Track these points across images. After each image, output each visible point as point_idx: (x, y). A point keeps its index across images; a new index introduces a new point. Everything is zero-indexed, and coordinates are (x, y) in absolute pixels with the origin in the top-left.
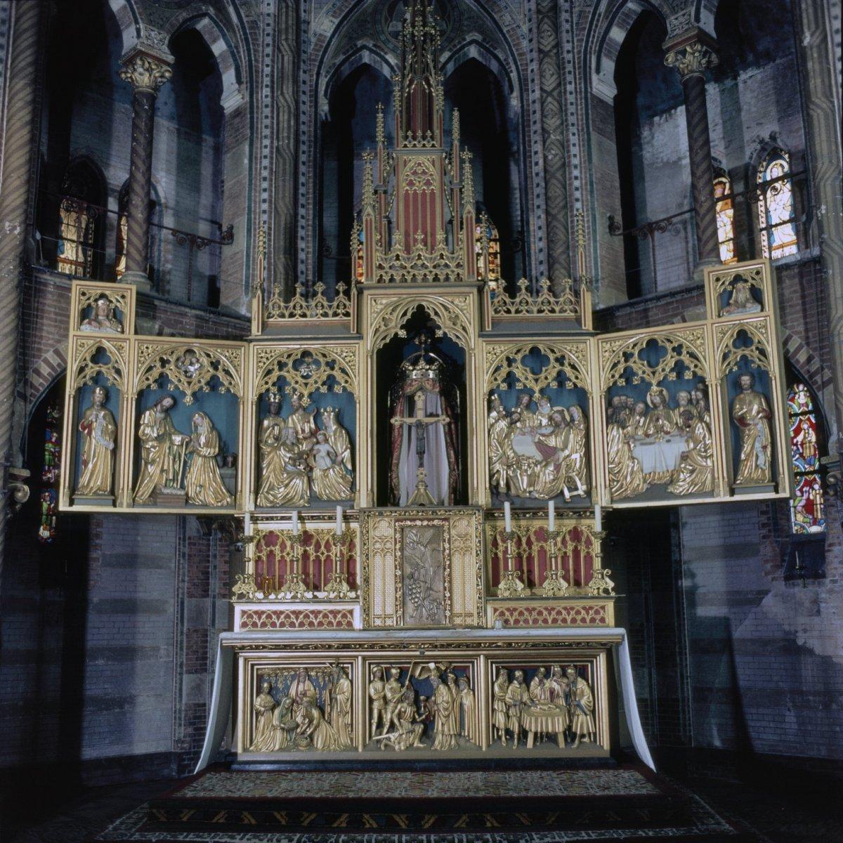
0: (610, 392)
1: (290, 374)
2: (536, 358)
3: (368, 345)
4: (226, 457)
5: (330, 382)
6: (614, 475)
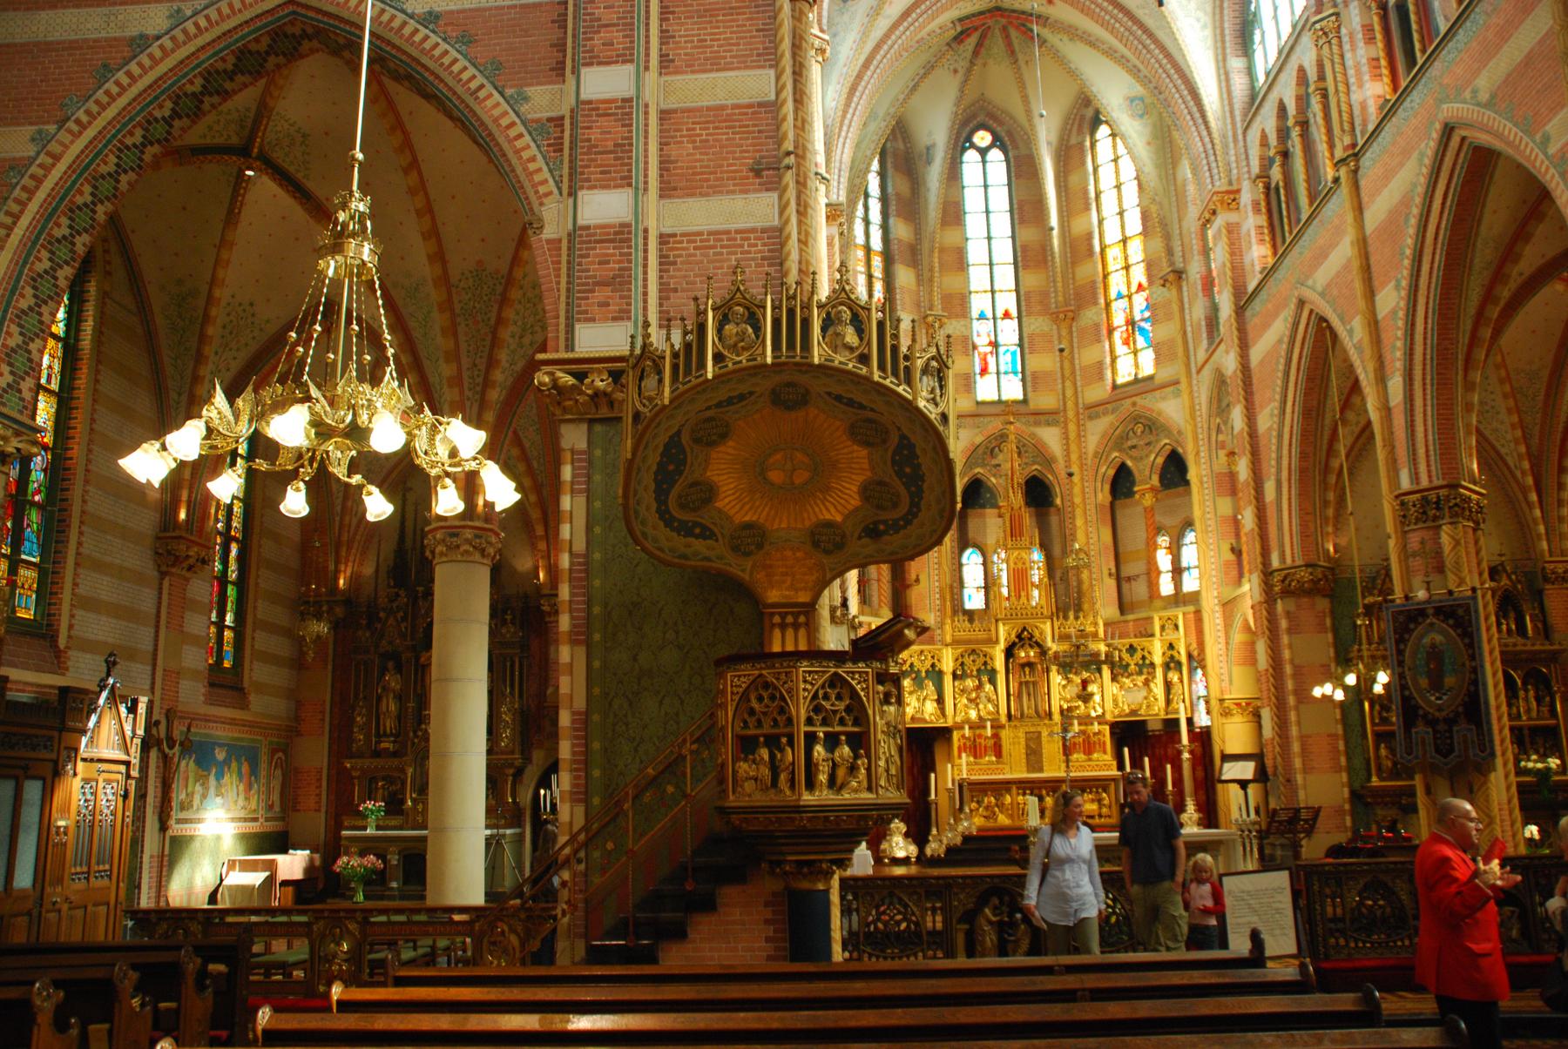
3: (1002, 645)
4: (940, 701)
5: (985, 663)
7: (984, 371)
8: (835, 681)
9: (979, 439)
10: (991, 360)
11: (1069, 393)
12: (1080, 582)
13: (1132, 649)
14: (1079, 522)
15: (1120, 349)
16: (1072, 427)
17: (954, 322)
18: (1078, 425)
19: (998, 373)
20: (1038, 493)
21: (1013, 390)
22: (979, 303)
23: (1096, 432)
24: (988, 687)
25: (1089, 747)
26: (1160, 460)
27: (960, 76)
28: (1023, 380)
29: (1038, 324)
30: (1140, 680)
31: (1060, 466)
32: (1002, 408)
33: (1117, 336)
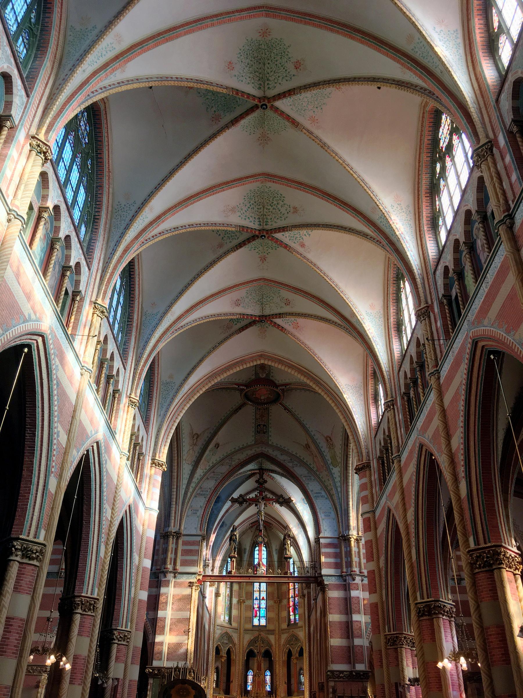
7: (256, 616)
12: (276, 686)
16: (277, 636)
18: (279, 635)
19: (259, 617)
20: (268, 655)
21: (263, 622)
22: (256, 595)
23: (284, 637)
26: (299, 649)
27: (253, 533)
28: (266, 619)
29: (271, 603)
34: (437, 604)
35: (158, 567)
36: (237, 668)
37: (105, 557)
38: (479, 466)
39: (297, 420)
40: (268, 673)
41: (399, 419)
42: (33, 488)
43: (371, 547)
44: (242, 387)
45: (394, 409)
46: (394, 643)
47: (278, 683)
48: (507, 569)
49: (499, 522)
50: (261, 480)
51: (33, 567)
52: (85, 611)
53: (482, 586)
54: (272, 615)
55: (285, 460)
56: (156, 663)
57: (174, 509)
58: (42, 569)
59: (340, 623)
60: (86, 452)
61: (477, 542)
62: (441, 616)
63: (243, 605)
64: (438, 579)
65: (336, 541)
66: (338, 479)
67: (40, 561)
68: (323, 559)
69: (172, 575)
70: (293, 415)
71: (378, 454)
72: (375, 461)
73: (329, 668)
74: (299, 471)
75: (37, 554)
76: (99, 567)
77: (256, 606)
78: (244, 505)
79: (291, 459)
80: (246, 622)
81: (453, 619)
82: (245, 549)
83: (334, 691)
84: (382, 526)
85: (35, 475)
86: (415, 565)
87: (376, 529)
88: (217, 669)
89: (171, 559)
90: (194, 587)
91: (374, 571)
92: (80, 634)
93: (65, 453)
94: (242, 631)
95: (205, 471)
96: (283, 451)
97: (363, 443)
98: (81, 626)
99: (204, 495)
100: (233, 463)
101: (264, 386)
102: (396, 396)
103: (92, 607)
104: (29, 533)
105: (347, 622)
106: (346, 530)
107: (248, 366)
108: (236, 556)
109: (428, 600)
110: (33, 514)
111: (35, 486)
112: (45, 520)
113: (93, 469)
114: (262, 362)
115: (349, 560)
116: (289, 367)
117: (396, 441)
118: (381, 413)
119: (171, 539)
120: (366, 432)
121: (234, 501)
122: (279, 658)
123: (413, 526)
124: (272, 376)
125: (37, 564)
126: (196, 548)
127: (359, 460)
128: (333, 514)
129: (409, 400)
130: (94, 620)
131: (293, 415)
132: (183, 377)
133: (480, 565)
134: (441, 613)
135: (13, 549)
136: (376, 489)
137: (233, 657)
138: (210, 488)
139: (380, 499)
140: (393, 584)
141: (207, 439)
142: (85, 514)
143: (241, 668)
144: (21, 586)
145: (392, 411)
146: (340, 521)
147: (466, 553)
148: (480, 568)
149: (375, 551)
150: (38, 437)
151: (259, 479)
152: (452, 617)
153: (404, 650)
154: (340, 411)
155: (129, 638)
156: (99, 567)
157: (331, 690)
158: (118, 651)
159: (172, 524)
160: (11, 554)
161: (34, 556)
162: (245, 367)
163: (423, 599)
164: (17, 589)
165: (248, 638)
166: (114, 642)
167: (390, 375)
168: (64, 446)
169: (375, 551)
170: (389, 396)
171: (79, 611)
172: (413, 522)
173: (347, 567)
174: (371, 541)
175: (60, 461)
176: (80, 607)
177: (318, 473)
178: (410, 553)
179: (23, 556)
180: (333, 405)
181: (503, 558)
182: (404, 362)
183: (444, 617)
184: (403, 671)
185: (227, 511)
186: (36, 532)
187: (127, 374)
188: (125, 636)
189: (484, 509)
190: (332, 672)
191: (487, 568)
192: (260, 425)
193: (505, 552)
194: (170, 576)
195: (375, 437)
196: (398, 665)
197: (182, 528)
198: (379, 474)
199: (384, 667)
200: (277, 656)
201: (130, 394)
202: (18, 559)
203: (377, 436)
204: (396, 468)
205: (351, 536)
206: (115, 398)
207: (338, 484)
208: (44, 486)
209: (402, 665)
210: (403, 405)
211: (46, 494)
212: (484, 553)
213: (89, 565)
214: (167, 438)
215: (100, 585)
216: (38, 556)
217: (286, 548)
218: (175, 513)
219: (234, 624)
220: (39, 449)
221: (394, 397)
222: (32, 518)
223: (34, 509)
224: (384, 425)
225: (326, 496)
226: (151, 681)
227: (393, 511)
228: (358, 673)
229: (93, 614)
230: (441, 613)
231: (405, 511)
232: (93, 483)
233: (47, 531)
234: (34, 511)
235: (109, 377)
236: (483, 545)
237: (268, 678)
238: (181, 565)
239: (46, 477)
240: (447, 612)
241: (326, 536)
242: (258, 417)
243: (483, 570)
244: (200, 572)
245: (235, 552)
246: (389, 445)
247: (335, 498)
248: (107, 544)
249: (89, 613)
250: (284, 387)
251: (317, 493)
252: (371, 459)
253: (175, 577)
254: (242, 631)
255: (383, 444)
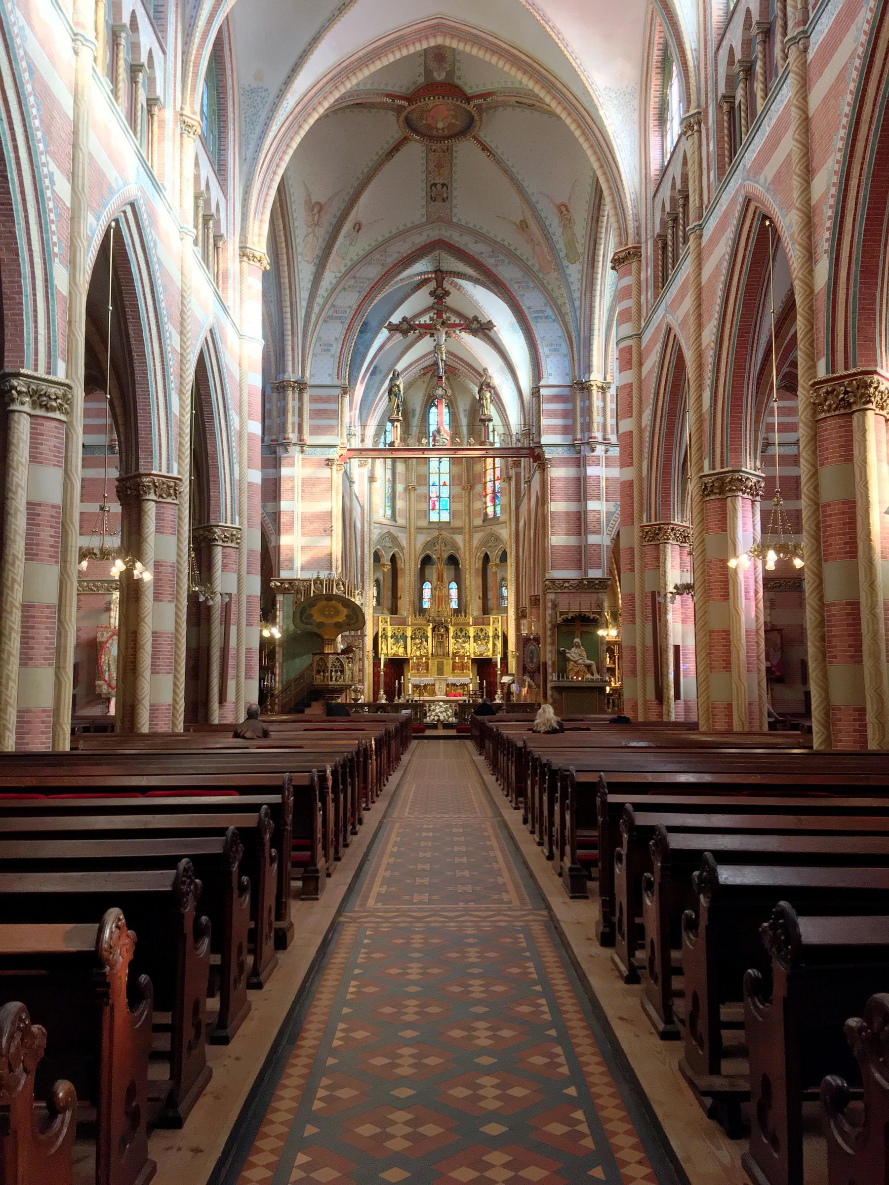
0: (474, 637)
1: (417, 632)
2: (461, 630)
4: (405, 648)
6: (474, 653)
8: (337, 659)
9: (428, 540)
10: (437, 504)
11: (467, 521)
13: (482, 630)
14: (467, 576)
15: (489, 504)
16: (467, 535)
17: (422, 488)
20: (453, 561)
21: (445, 517)
22: (434, 479)
23: (477, 537)
24: (425, 643)
25: (463, 667)
26: (500, 553)
29: (457, 489)
30: (484, 642)
31: (462, 551)
32: (440, 525)
33: (488, 498)
34: (737, 476)
35: (274, 437)
36: (407, 579)
37: (181, 414)
38: (860, 226)
39: (506, 171)
40: (454, 585)
41: (708, 152)
42: (26, 283)
43: (630, 395)
44: (399, 102)
45: (700, 131)
46: (655, 537)
47: (468, 598)
48: (877, 411)
49: (878, 330)
50: (439, 291)
51: (55, 424)
52: (161, 496)
53: (827, 439)
54: (459, 506)
55: (482, 253)
56: (284, 574)
57: (290, 343)
58: (73, 426)
59: (567, 513)
60: (113, 224)
61: (832, 366)
62: (740, 494)
63: (412, 493)
64: (743, 438)
65: (566, 391)
66: (576, 286)
67: (67, 413)
68: (545, 422)
69: (298, 448)
70: (498, 162)
71: (657, 230)
72: (650, 244)
73: (548, 576)
74: (507, 272)
75: (59, 401)
76: (174, 430)
77: (433, 495)
78: (411, 335)
79: (493, 251)
80: (418, 517)
81: (758, 498)
82: (414, 411)
83: (555, 606)
84: (652, 360)
85: (23, 259)
86: (707, 417)
87: (641, 364)
88: (377, 583)
89: (293, 424)
90: (334, 467)
91: (631, 432)
92: (159, 530)
93: (72, 219)
94: (413, 530)
95: (339, 275)
96: (479, 236)
97: (630, 211)
98: (159, 517)
99: (340, 318)
100: (389, 260)
101: (443, 97)
102: (707, 103)
103: (172, 491)
104: (36, 365)
105: (579, 513)
106: (584, 374)
107: (412, 50)
108: (401, 418)
109: (723, 470)
110: (36, 332)
111: (29, 281)
112: (61, 343)
113: (134, 256)
114: (440, 41)
115: (587, 420)
116: (494, 53)
117: (697, 197)
118: (669, 148)
119: (290, 393)
120: (638, 188)
121: (393, 328)
122: (470, 565)
123: (711, 352)
124: (459, 78)
125: (63, 418)
126: (333, 406)
127: (621, 243)
128: (564, 348)
129: (732, 111)
130: (179, 509)
131: (498, 162)
132: (282, 77)
133: (830, 406)
134: (742, 490)
135: (14, 392)
136: (648, 295)
137: (400, 565)
138: (350, 307)
139: (655, 311)
140: (662, 452)
141: (338, 214)
142: (133, 341)
143: (413, 579)
144: (42, 453)
145: (696, 135)
146: (576, 358)
147: (807, 387)
148: (829, 411)
149: (635, 400)
150: (13, 184)
151: (436, 290)
152: (757, 495)
153: (669, 546)
154: (592, 146)
155: (239, 539)
156: (174, 430)
157: (550, 605)
158: (224, 556)
159: (290, 369)
160: (13, 400)
161: (54, 404)
162: (405, 52)
163: (714, 469)
164: (34, 458)
165: (421, 539)
166: (216, 543)
167: (698, 59)
168: (69, 205)
169: (635, 400)
170: (693, 104)
171: (152, 496)
172: (713, 345)
173: (582, 432)
174: (630, 385)
175: (66, 232)
176: (152, 491)
177: (541, 275)
178: (700, 397)
179: (34, 404)
180: (577, 133)
181: (874, 393)
182: (731, 26)
183: (745, 496)
184: (665, 576)
185: (381, 347)
186: (49, 363)
187: (170, 64)
188: (232, 535)
189: (854, 308)
190: (553, 581)
191: (842, 411)
192: (435, 185)
193: (879, 383)
194: (294, 451)
195: (654, 197)
196: (657, 568)
197: (307, 374)
198: (656, 266)
199: (636, 571)
200: (467, 562)
201: (182, 109)
202: (27, 408)
203: (659, 195)
204: (691, 250)
205: (592, 383)
206: (152, 116)
207: (576, 295)
208: (46, 280)
209: (665, 567)
210: (719, 123)
211: (52, 295)
212: (842, 384)
213: (157, 427)
214: (264, 207)
215: (180, 457)
216: (61, 405)
217: (482, 405)
218: (293, 349)
219: (401, 521)
220: (20, 207)
221: (703, 106)
222: (36, 339)
223: (36, 322)
224: (676, 170)
225: (553, 317)
226: (280, 598)
227: (677, 330)
228: (591, 581)
229: (175, 502)
230: (742, 490)
231: (700, 326)
232: (137, 284)
233: (69, 362)
234: (36, 327)
235: (134, 69)
236: (841, 372)
237: (454, 593)
238: (311, 434)
239: (45, 264)
240: (751, 488)
241: (550, 383)
242: (432, 166)
243: (833, 413)
244: (342, 444)
245: (398, 412)
246: (681, 209)
247: (569, 318)
248: (181, 393)
249: (169, 500)
250: (481, 101)
251: (537, 312)
252: (643, 239)
253: (302, 452)
254: (413, 530)
255: (668, 209)
